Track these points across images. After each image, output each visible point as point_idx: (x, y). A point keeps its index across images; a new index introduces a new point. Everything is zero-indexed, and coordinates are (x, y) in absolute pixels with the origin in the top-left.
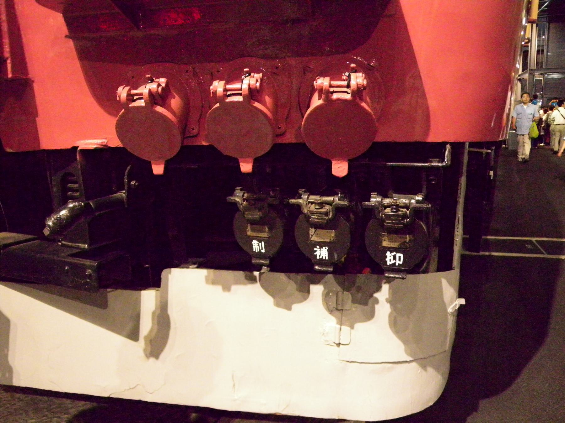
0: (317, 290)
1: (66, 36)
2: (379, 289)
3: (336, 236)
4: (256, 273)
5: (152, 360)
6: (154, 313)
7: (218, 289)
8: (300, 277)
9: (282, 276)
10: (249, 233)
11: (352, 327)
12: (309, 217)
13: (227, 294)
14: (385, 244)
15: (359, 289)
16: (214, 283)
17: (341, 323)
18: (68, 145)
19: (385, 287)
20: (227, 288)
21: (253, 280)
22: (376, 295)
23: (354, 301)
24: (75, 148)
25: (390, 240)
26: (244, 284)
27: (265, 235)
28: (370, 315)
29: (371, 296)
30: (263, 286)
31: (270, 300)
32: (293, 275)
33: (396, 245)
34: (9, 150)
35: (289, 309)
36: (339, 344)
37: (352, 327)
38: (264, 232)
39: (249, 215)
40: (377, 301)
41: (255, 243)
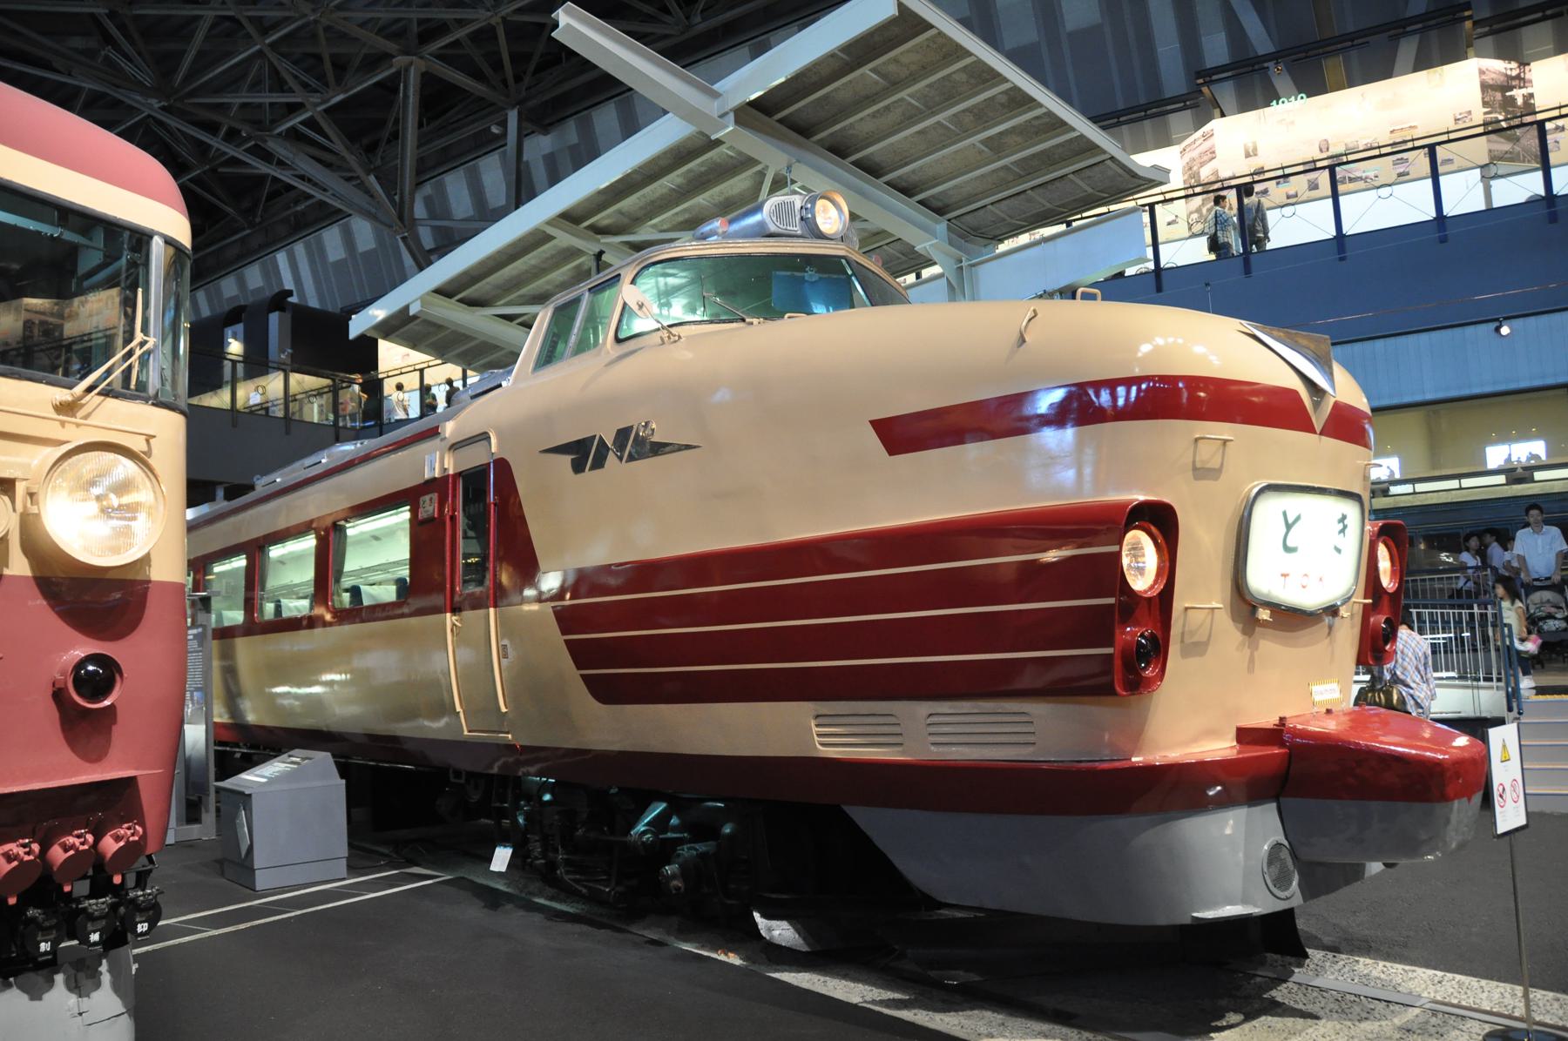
0: (59, 978)
2: (100, 964)
3: (107, 923)
8: (45, 972)
12: (93, 913)
14: (137, 920)
15: (88, 967)
19: (104, 961)
22: (100, 969)
23: (87, 978)
25: (141, 916)
28: (98, 985)
29: (97, 970)
36: (80, 1014)
38: (52, 934)
39: (47, 924)
40: (101, 973)
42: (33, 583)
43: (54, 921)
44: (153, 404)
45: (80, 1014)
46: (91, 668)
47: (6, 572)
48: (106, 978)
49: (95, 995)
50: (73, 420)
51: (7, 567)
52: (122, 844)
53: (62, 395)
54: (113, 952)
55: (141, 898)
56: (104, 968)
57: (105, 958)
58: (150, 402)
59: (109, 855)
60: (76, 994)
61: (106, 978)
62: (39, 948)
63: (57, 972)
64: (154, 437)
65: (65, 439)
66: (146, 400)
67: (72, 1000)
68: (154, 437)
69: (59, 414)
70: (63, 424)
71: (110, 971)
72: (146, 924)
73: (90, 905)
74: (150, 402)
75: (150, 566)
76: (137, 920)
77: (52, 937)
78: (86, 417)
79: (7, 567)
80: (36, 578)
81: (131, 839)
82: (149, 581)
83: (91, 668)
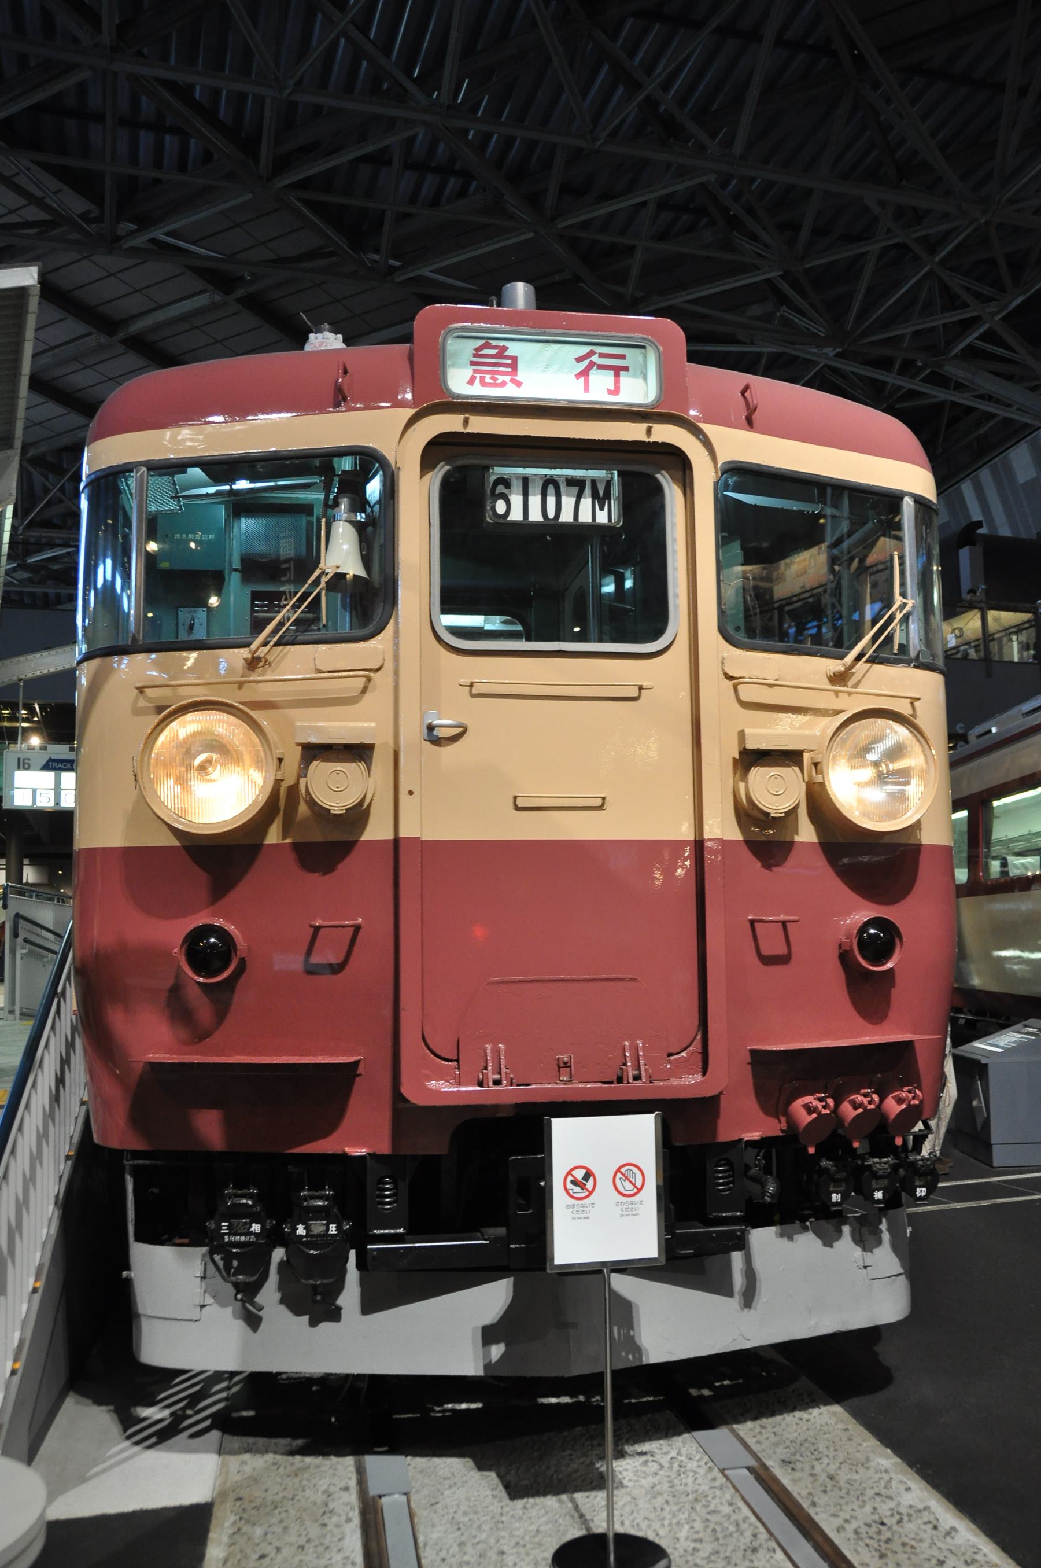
0: (846, 1229)
1: (749, 1063)
2: (880, 1222)
4: (808, 1223)
5: (746, 1310)
6: (742, 1270)
7: (785, 1240)
8: (834, 1221)
9: (823, 1222)
10: (831, 1189)
11: (872, 1252)
12: (877, 1172)
13: (791, 1243)
16: (782, 1235)
17: (864, 1249)
18: (736, 1138)
19: (884, 1220)
20: (790, 1238)
21: (805, 1229)
22: (881, 1227)
24: (741, 1140)
25: (920, 1181)
26: (801, 1233)
27: (842, 1189)
28: (879, 1243)
29: (878, 1228)
30: (815, 1232)
31: (819, 1242)
32: (830, 1220)
33: (922, 1184)
34: (678, 1144)
35: (831, 1246)
36: (865, 1267)
37: (872, 1252)
39: (838, 1176)
40: (881, 1231)
41: (834, 1195)
42: (818, 847)
43: (844, 1174)
44: (915, 667)
45: (865, 1267)
46: (872, 931)
47: (797, 839)
48: (886, 1236)
49: (876, 1251)
50: (845, 689)
51: (797, 834)
52: (904, 1106)
53: (835, 666)
54: (891, 1212)
55: (920, 1163)
56: (884, 1226)
57: (884, 1216)
58: (912, 665)
59: (892, 1117)
60: (860, 1246)
61: (886, 1236)
62: (831, 1198)
63: (845, 1224)
64: (919, 699)
65: (839, 708)
66: (908, 663)
67: (858, 1252)
68: (919, 699)
69: (833, 685)
70: (837, 693)
71: (888, 1230)
72: (924, 1189)
73: (874, 1163)
74: (912, 665)
75: (920, 830)
76: (917, 1183)
77: (842, 1189)
78: (856, 685)
79: (797, 834)
80: (820, 843)
81: (912, 1102)
82: (920, 845)
83: (872, 931)
